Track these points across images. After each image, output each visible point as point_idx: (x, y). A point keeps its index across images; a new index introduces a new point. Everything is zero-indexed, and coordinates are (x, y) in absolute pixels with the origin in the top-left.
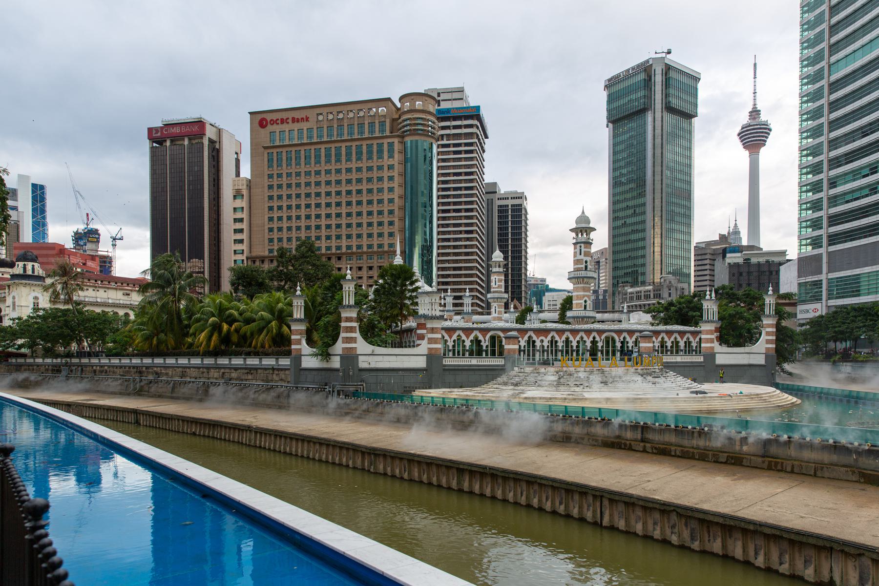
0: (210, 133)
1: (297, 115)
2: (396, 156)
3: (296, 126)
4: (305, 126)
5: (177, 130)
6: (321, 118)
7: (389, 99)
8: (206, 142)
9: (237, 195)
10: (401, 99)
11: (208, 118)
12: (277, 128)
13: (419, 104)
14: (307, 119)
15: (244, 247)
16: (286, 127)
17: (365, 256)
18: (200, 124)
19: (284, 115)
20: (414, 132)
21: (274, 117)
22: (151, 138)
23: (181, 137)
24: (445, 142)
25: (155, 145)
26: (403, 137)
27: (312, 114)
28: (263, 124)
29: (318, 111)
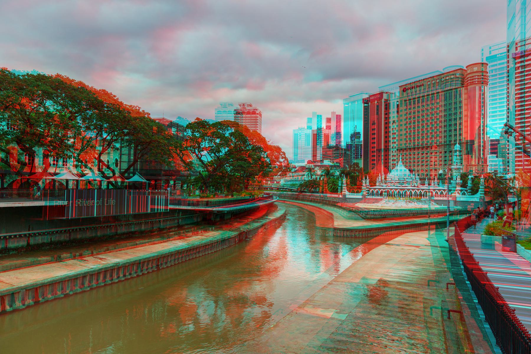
0: (385, 96)
1: (418, 84)
2: (463, 96)
3: (418, 89)
4: (422, 88)
5: (373, 98)
6: (429, 83)
7: (461, 69)
8: (383, 101)
9: (394, 122)
10: (467, 67)
11: (385, 90)
12: (409, 91)
13: (475, 69)
14: (423, 85)
15: (395, 145)
16: (413, 90)
17: (448, 146)
18: (381, 94)
19: (413, 85)
20: (472, 83)
21: (409, 86)
22: (364, 103)
23: (374, 100)
24: (520, 70)
25: (365, 105)
26: (467, 86)
27: (425, 83)
28: (404, 90)
29: (427, 80)
